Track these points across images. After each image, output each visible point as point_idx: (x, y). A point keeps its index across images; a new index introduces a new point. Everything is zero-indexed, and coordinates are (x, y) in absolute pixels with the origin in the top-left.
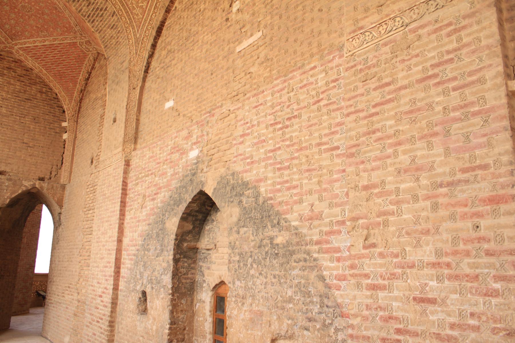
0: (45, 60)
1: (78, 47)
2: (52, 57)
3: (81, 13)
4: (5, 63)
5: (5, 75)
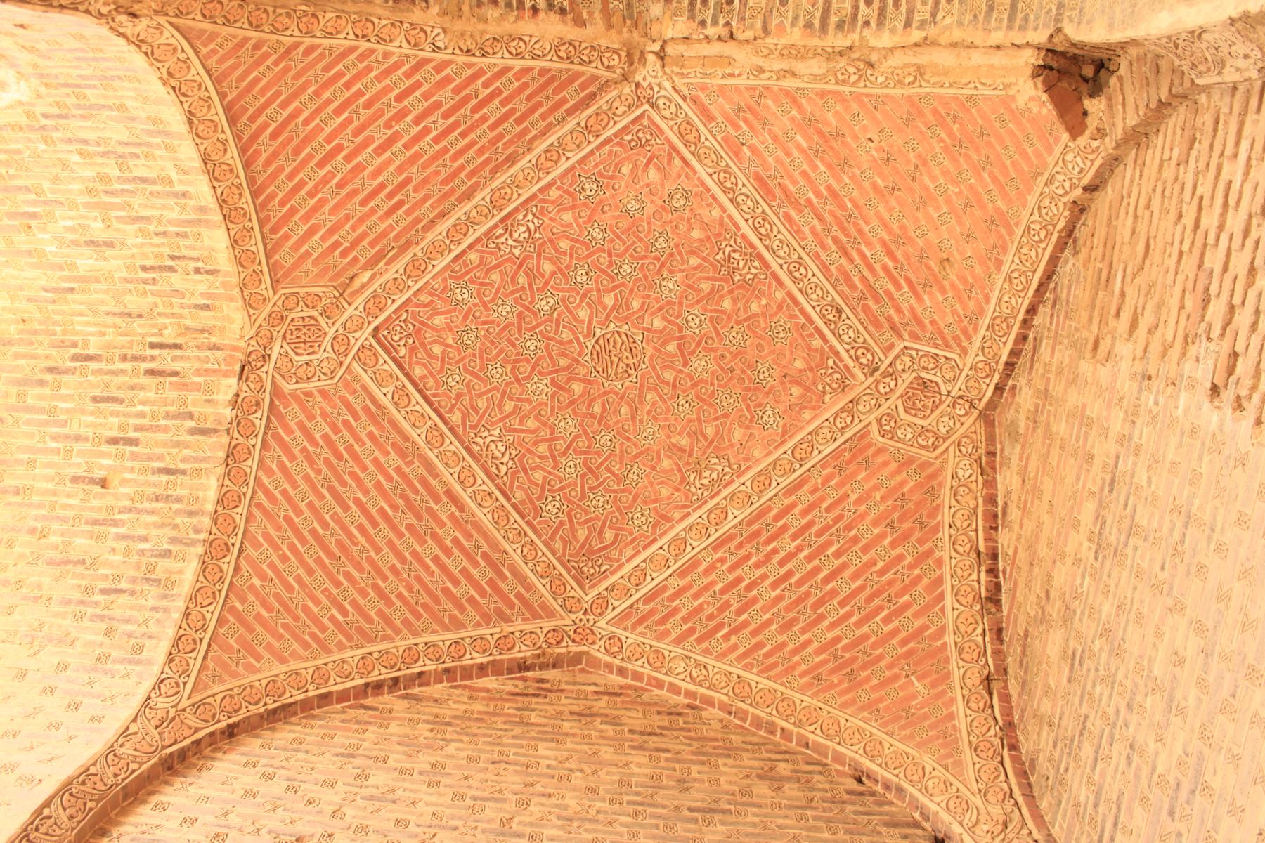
0: (745, 624)
1: (880, 451)
2: (774, 586)
3: (834, 20)
4: (564, 701)
5: (567, 734)
